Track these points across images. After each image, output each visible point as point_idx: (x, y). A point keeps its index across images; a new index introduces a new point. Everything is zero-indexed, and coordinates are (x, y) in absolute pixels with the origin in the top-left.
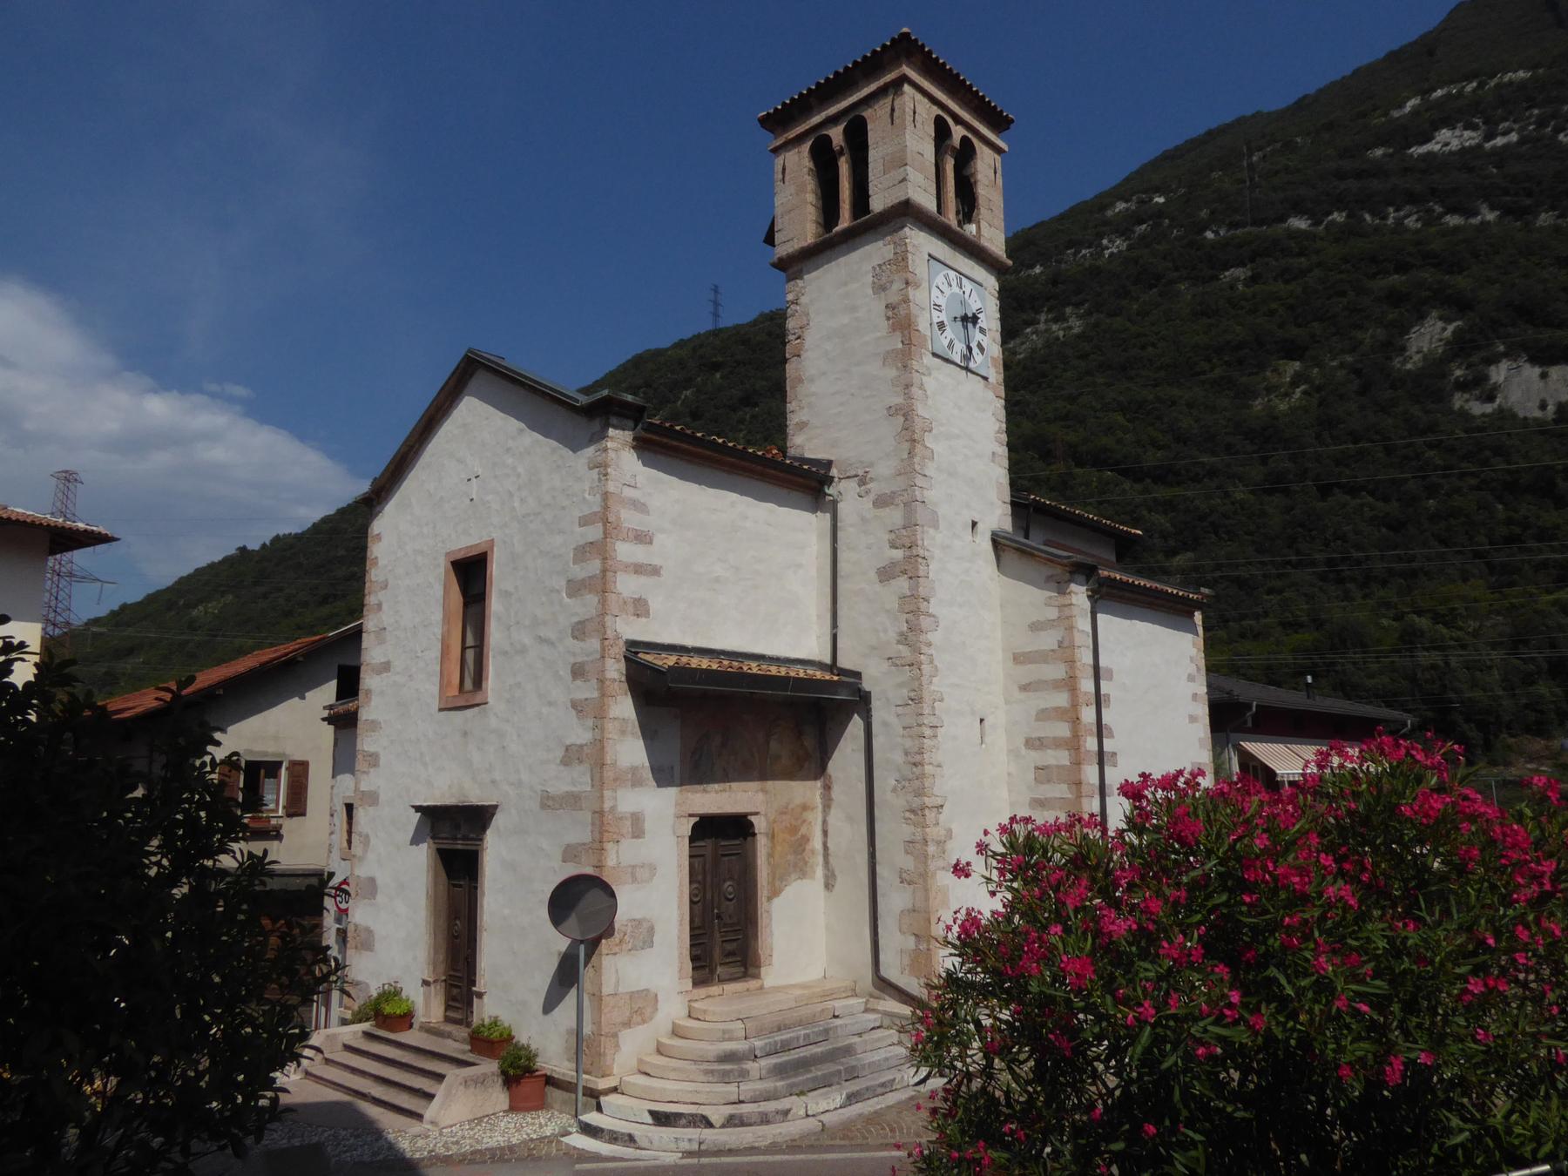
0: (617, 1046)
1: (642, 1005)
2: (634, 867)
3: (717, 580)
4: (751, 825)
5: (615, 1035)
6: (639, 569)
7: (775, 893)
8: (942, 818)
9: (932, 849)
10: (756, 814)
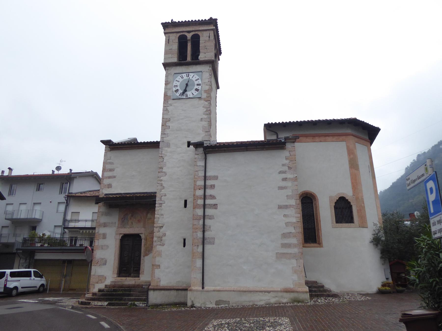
0: (94, 288)
1: (102, 278)
2: (102, 246)
3: (133, 176)
4: (140, 236)
5: (94, 285)
6: (109, 177)
7: (146, 255)
8: (162, 230)
9: (155, 239)
10: (142, 233)
